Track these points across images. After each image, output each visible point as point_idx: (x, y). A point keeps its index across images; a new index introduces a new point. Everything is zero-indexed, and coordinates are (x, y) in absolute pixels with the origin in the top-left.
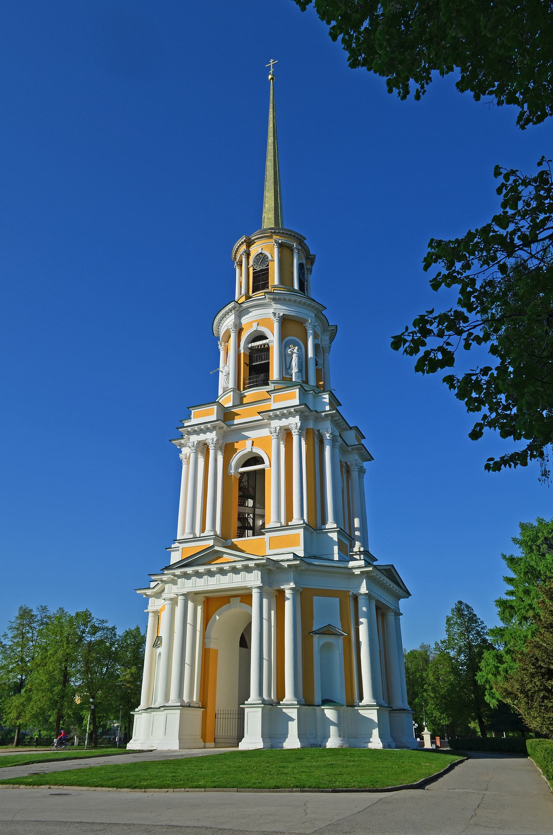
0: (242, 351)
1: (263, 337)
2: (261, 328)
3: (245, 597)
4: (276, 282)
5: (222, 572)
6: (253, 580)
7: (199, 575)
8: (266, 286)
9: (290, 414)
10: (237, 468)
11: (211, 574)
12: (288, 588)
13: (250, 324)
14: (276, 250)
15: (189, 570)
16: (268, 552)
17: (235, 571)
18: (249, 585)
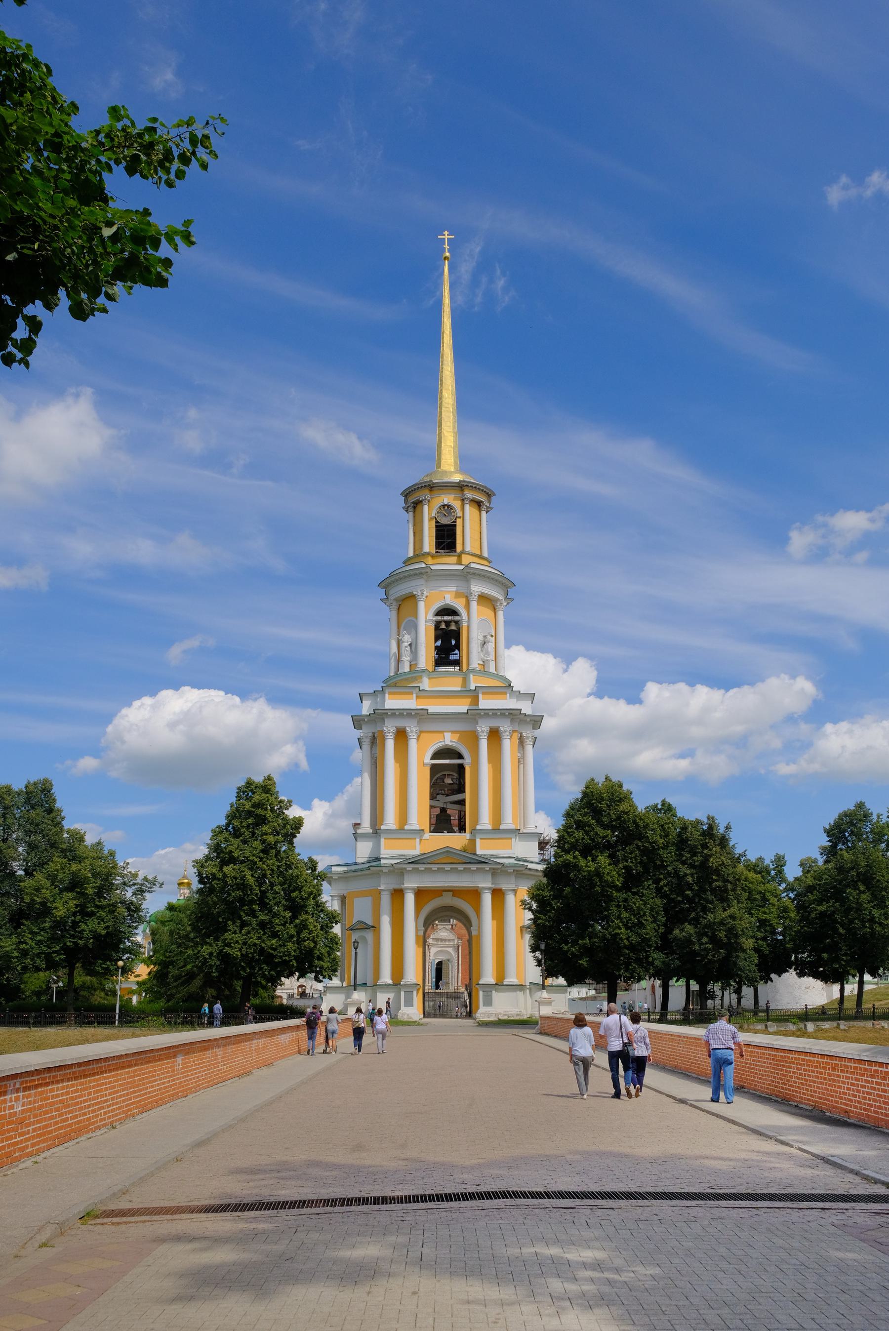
10: (433, 758)
15: (422, 867)
18: (481, 885)
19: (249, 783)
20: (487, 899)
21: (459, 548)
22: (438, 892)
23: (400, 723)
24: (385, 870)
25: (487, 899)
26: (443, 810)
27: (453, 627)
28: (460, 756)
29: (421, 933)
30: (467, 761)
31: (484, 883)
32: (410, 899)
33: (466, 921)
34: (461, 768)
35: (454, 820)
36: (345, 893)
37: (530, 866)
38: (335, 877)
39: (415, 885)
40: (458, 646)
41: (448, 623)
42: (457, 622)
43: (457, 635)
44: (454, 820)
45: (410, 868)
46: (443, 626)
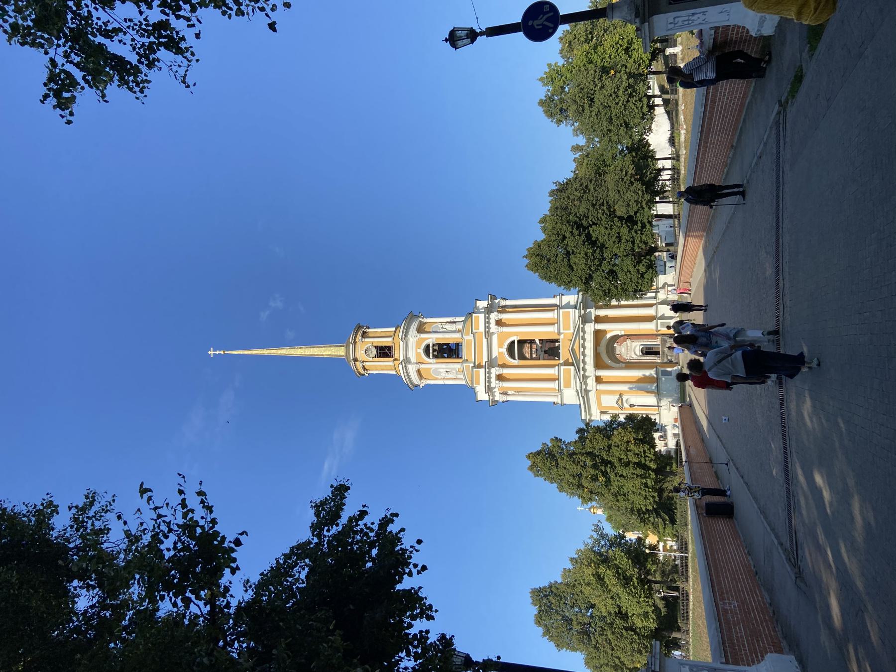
0: (434, 361)
1: (428, 346)
2: (423, 346)
3: (598, 334)
4: (390, 339)
5: (584, 347)
6: (590, 328)
7: (584, 362)
8: (390, 348)
9: (489, 318)
11: (584, 354)
12: (594, 312)
13: (418, 354)
14: (367, 340)
15: (582, 365)
16: (572, 331)
17: (584, 339)
19: (531, 468)
20: (600, 327)
21: (390, 345)
22: (597, 355)
23: (493, 379)
24: (584, 387)
25: (600, 327)
26: (546, 352)
27: (436, 348)
28: (513, 342)
29: (624, 365)
30: (516, 339)
31: (590, 328)
32: (602, 373)
33: (615, 338)
34: (519, 341)
35: (551, 345)
36: (598, 412)
37: (580, 300)
38: (588, 417)
39: (593, 369)
40: (447, 344)
41: (434, 350)
42: (434, 345)
43: (439, 345)
44: (551, 345)
45: (582, 372)
46: (436, 353)
